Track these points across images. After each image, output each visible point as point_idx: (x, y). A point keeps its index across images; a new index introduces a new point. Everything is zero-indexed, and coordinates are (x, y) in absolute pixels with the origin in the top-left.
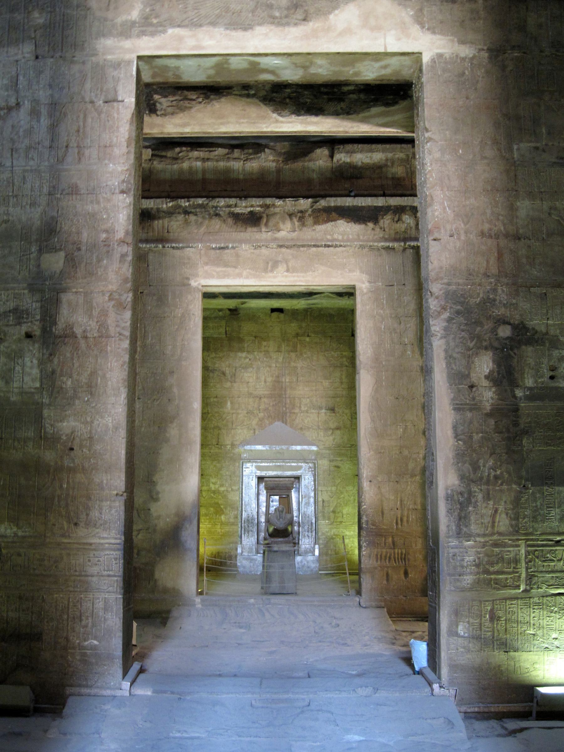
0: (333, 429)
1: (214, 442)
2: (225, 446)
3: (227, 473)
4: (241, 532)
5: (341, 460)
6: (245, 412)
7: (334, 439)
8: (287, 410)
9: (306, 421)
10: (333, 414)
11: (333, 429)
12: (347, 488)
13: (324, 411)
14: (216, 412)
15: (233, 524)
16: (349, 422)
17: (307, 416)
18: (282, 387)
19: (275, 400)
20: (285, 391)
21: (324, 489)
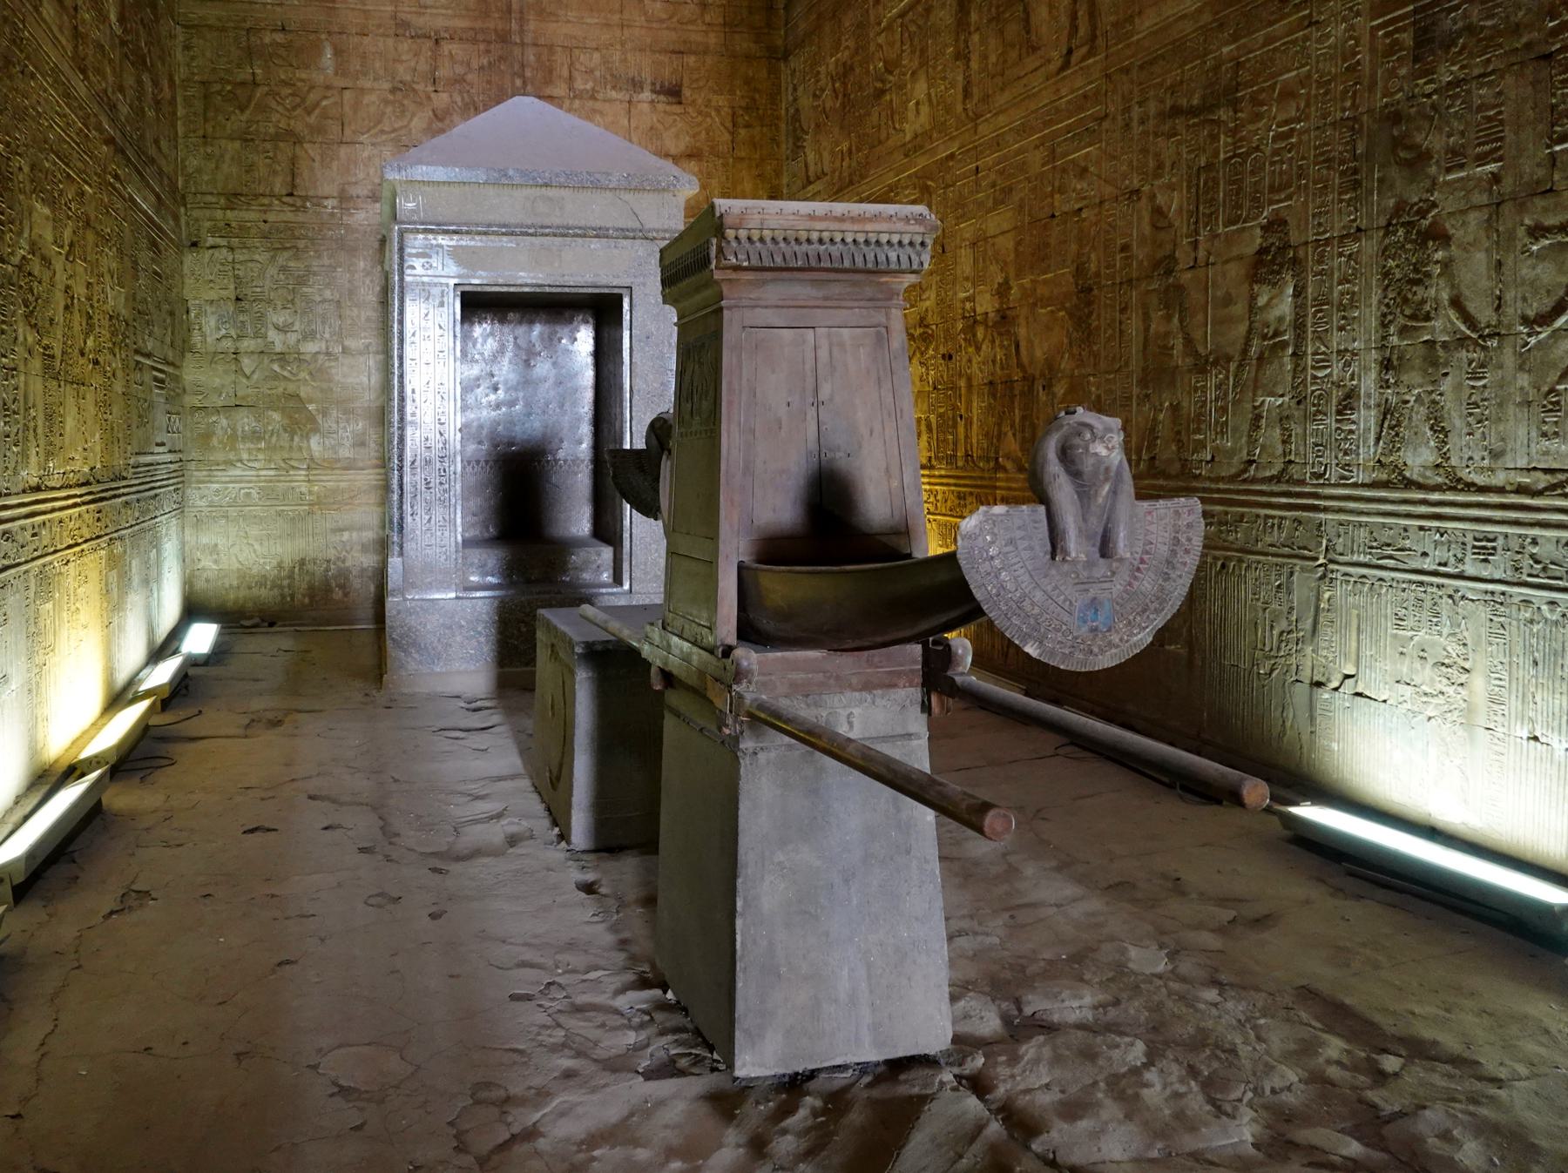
1: (279, 186)
2: (319, 201)
3: (328, 294)
4: (401, 508)
6: (387, 86)
8: (529, 87)
10: (678, 109)
13: (647, 95)
14: (285, 83)
15: (350, 466)
16: (727, 137)
17: (594, 111)
18: (509, 11)
19: (488, 51)
20: (522, 20)
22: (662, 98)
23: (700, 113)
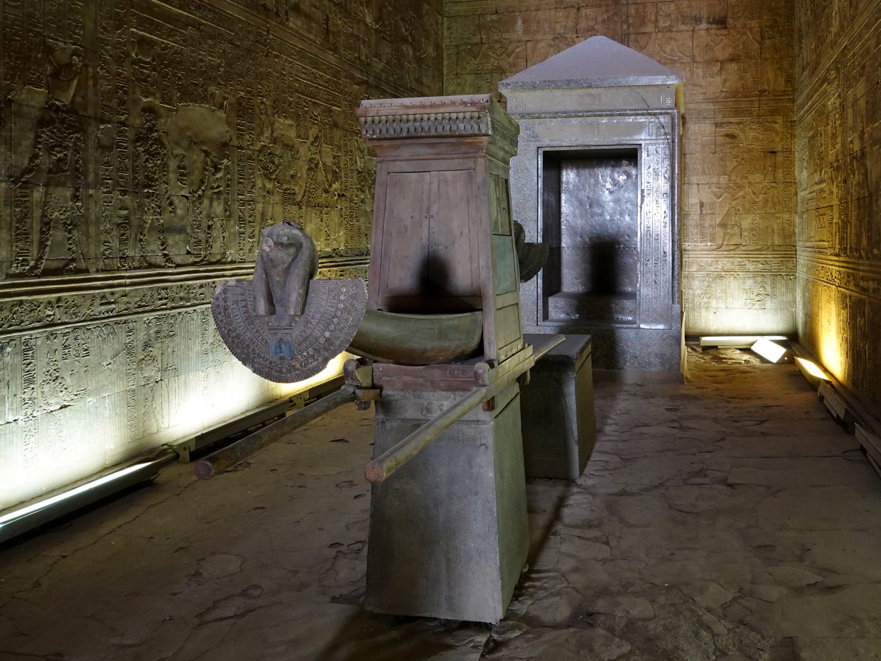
0: (721, 62)
5: (738, 123)
7: (725, 81)
8: (631, 29)
9: (668, 50)
10: (724, 32)
11: (721, 62)
12: (752, 178)
13: (704, 25)
16: (757, 46)
17: (671, 38)
19: (608, 11)
21: (703, 179)
22: (714, 26)
23: (738, 33)
